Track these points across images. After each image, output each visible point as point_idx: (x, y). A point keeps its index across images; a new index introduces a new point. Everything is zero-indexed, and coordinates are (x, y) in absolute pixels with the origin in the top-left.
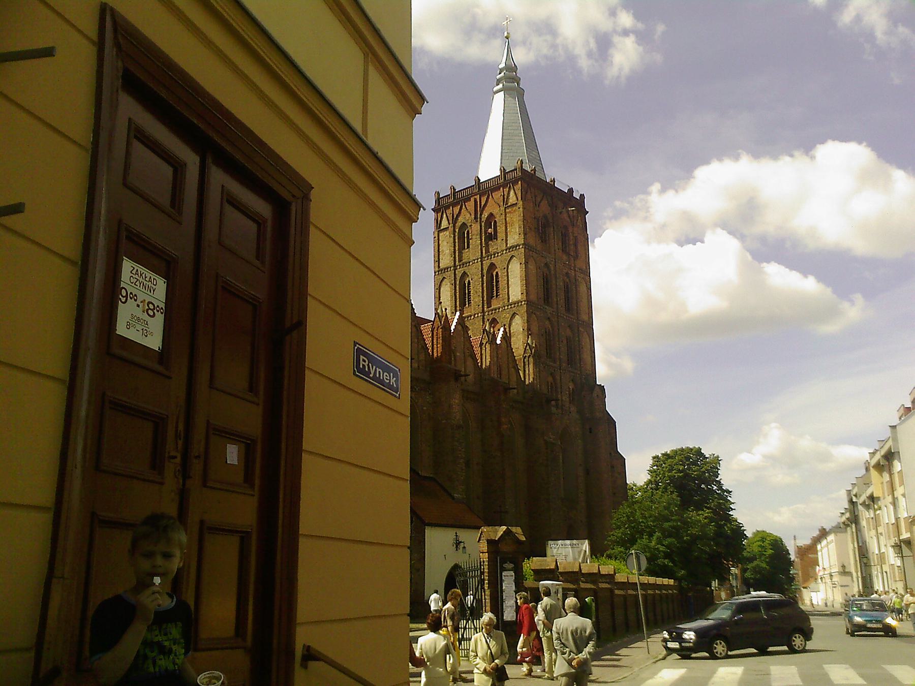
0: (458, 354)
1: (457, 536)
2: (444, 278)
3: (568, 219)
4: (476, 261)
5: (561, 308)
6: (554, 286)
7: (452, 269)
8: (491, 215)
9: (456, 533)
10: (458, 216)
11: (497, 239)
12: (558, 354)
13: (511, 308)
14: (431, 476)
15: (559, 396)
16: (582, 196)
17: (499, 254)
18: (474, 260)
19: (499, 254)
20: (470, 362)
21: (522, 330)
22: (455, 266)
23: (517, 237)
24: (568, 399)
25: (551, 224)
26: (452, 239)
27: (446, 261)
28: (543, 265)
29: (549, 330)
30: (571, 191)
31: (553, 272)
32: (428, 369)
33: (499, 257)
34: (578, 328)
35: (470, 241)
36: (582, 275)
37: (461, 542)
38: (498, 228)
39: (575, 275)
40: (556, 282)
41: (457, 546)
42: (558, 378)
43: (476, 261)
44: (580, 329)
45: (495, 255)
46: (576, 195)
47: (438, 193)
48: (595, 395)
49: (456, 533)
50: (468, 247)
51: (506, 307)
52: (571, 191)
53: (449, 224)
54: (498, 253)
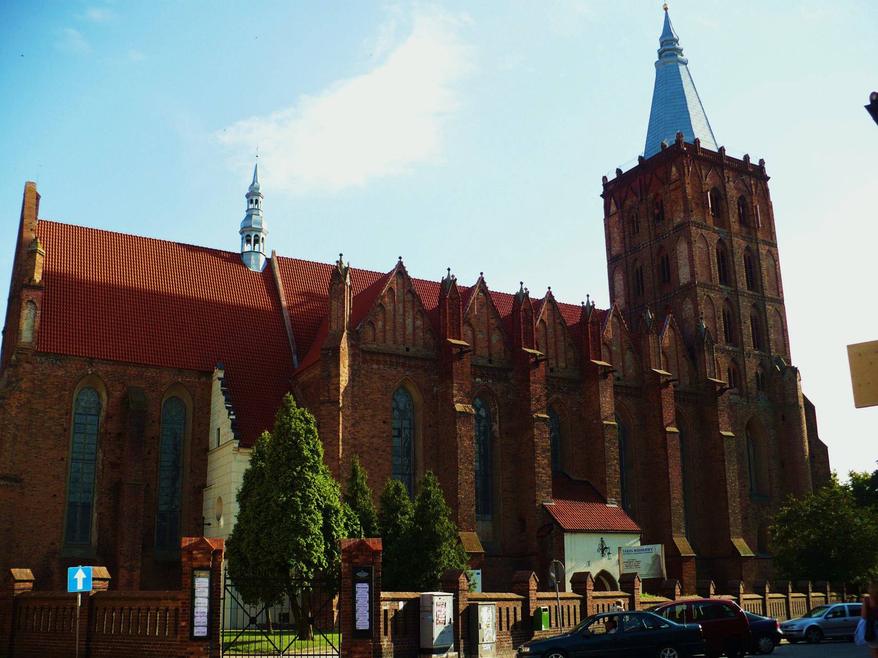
0: (614, 348)
1: (602, 541)
2: (617, 266)
3: (745, 189)
4: (645, 245)
5: (741, 287)
6: (731, 263)
7: (623, 255)
8: (657, 195)
9: (602, 539)
10: (625, 200)
11: (663, 219)
12: (740, 337)
13: (682, 291)
14: (585, 479)
15: (744, 383)
16: (762, 162)
17: (667, 235)
18: (643, 244)
19: (667, 235)
20: (629, 356)
21: (694, 315)
22: (626, 252)
23: (682, 215)
24: (755, 387)
25: (723, 196)
26: (621, 224)
27: (617, 248)
28: (716, 242)
29: (728, 312)
30: (747, 157)
31: (729, 248)
32: (578, 367)
33: (668, 238)
34: (765, 306)
35: (639, 224)
36: (767, 248)
37: (606, 548)
38: (664, 207)
39: (758, 249)
40: (733, 258)
41: (603, 553)
42: (741, 362)
43: (645, 245)
44: (767, 306)
45: (662, 236)
46: (754, 161)
47: (605, 178)
48: (786, 378)
49: (602, 539)
50: (638, 232)
51: (677, 292)
52: (747, 157)
53: (618, 208)
54: (666, 234)
